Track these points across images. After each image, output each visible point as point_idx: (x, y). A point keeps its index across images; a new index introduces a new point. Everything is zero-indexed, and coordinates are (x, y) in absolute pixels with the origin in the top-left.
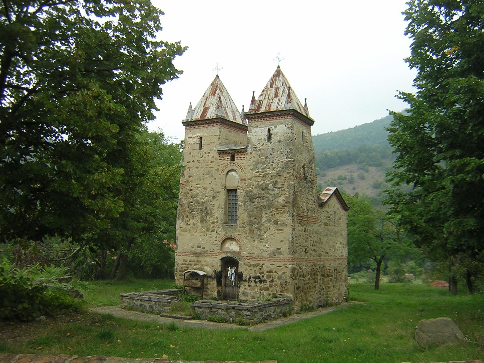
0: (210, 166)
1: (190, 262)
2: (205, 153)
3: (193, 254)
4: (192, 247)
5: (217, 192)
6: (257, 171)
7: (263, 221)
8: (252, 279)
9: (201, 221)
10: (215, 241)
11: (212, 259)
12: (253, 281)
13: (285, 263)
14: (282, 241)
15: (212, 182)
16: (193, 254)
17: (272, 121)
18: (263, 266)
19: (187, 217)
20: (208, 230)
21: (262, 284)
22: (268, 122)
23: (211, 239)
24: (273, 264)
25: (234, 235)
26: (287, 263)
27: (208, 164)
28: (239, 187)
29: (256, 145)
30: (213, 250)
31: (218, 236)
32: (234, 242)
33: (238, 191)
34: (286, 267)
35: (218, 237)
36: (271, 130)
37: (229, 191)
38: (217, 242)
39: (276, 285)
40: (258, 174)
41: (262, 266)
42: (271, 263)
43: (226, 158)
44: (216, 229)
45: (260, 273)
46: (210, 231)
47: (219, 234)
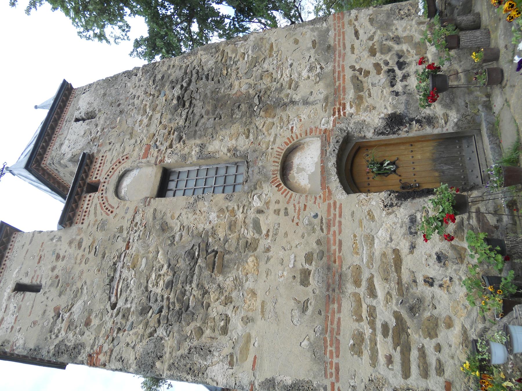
0: (87, 250)
1: (360, 319)
2: (53, 269)
3: (329, 300)
4: (304, 309)
5: (154, 218)
6: (138, 124)
7: (244, 88)
8: (399, 87)
9: (223, 269)
10: (286, 214)
11: (346, 220)
12: (405, 83)
13: (346, 26)
14: (296, 42)
15: (124, 241)
16: (329, 300)
17: (67, 117)
18: (357, 67)
19: (200, 331)
20: (250, 246)
21: (408, 61)
22: (65, 123)
23: (282, 231)
24: (353, 48)
25: (275, 154)
26: (346, 19)
27: (79, 257)
28: (159, 158)
29: (90, 138)
30: (317, 221)
31: (273, 207)
32: (297, 160)
33: (168, 161)
34: (356, 19)
35: (277, 207)
36: (79, 116)
37: (162, 191)
38: (291, 208)
39: (405, 28)
40: (145, 121)
41: (360, 70)
42: (350, 52)
43: (87, 202)
44: (252, 214)
45: (379, 73)
46: (256, 236)
47: (267, 203)
